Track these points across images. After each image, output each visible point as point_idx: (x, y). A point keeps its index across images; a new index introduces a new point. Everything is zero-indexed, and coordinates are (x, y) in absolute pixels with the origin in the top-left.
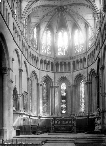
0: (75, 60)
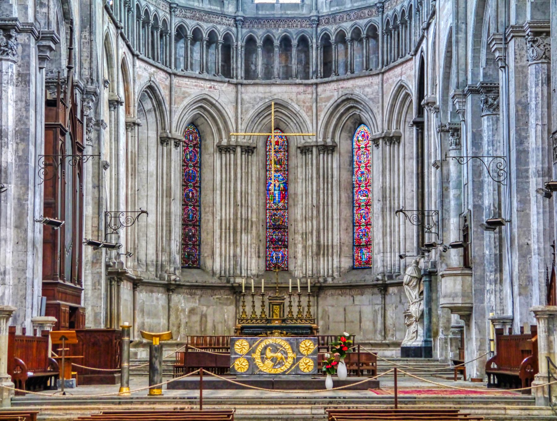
0: (332, 29)
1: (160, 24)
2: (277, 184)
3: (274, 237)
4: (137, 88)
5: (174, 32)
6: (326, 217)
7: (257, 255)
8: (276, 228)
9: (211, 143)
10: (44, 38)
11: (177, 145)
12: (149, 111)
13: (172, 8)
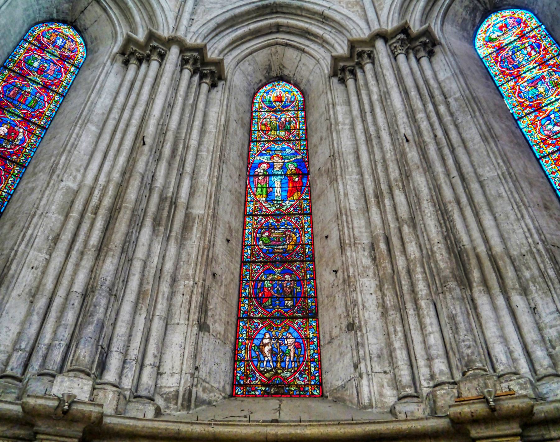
2: (278, 163)
3: (267, 284)
6: (454, 173)
7: (194, 316)
8: (272, 262)
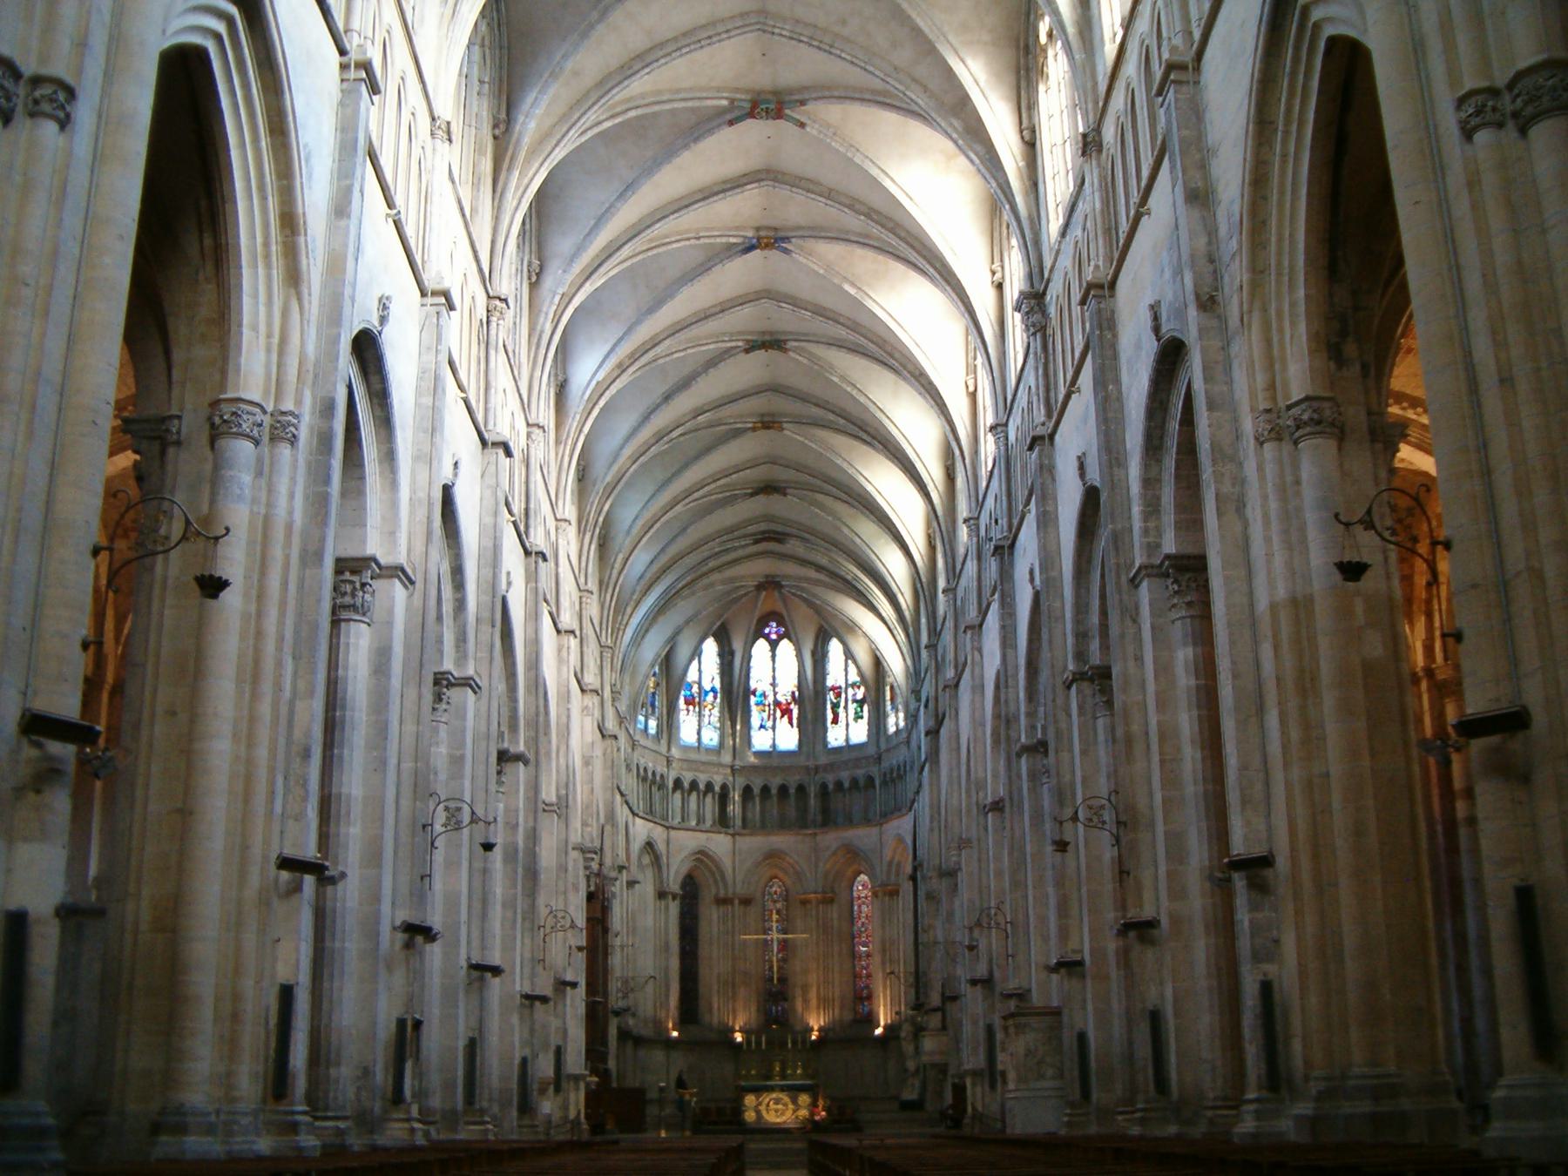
1: (658, 778)
4: (636, 846)
5: (671, 785)
9: (707, 895)
10: (590, 852)
11: (674, 898)
12: (647, 865)
13: (669, 762)
